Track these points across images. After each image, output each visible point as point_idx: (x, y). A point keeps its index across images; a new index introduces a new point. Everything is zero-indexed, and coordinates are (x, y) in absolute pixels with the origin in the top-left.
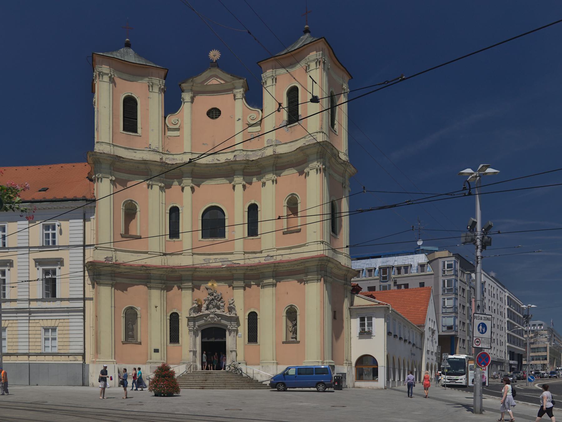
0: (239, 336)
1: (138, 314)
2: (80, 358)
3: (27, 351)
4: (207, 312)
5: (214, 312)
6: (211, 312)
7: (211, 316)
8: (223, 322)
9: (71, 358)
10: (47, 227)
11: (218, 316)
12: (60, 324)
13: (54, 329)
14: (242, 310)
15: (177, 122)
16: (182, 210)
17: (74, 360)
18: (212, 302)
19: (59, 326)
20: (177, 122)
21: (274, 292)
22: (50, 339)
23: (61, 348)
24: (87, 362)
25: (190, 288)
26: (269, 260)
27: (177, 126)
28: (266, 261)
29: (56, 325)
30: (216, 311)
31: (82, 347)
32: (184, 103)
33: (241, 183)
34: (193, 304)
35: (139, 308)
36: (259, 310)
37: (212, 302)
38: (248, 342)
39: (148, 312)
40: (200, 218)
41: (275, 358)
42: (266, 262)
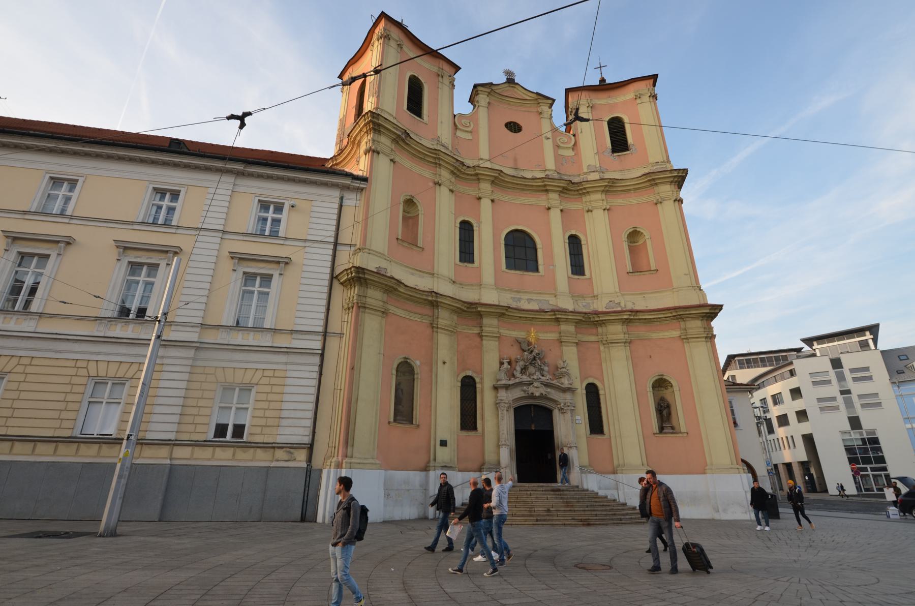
0: (577, 422)
1: (416, 372)
2: (302, 455)
3: (172, 436)
4: (525, 378)
5: (537, 379)
6: (534, 379)
7: (536, 384)
8: (554, 394)
9: (280, 454)
10: (264, 206)
11: (547, 385)
12: (265, 381)
13: (246, 389)
14: (579, 379)
15: (468, 125)
16: (479, 227)
17: (286, 459)
18: (534, 362)
19: (259, 383)
20: (468, 125)
21: (629, 354)
22: (233, 409)
23: (258, 430)
24: (317, 462)
25: (496, 337)
26: (613, 308)
27: (469, 129)
28: (607, 309)
29: (254, 381)
30: (540, 378)
31: (308, 432)
32: (479, 106)
33: (558, 207)
34: (502, 364)
35: (418, 363)
36: (602, 382)
37: (534, 362)
38: (589, 433)
39: (431, 371)
40: (503, 242)
41: (645, 462)
42: (607, 310)
